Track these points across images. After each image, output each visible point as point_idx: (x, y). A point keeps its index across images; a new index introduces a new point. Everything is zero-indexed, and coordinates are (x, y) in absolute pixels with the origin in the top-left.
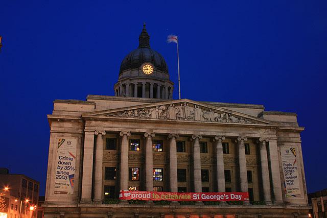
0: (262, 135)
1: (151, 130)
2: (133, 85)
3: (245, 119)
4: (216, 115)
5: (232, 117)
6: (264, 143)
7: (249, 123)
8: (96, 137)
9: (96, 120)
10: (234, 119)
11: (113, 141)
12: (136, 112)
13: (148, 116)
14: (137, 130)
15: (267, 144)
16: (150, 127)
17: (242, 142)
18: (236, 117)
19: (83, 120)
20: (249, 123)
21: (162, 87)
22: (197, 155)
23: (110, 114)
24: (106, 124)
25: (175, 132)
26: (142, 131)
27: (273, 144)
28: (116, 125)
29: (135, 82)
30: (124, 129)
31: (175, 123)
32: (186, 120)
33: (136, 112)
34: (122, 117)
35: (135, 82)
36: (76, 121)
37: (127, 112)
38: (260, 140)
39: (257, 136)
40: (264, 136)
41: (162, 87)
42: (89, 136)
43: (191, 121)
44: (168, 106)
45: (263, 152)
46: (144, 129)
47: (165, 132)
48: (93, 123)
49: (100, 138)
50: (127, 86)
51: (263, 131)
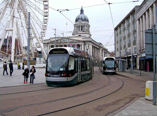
0: (80, 43)
7: (77, 41)
8: (50, 46)
10: (75, 41)
15: (81, 45)
19: (47, 44)
20: (77, 41)
21: (84, 26)
24: (51, 44)
27: (83, 46)
29: (77, 25)
34: (53, 42)
35: (77, 25)
36: (47, 44)
41: (84, 26)
45: (81, 47)
48: (49, 44)
49: (50, 47)
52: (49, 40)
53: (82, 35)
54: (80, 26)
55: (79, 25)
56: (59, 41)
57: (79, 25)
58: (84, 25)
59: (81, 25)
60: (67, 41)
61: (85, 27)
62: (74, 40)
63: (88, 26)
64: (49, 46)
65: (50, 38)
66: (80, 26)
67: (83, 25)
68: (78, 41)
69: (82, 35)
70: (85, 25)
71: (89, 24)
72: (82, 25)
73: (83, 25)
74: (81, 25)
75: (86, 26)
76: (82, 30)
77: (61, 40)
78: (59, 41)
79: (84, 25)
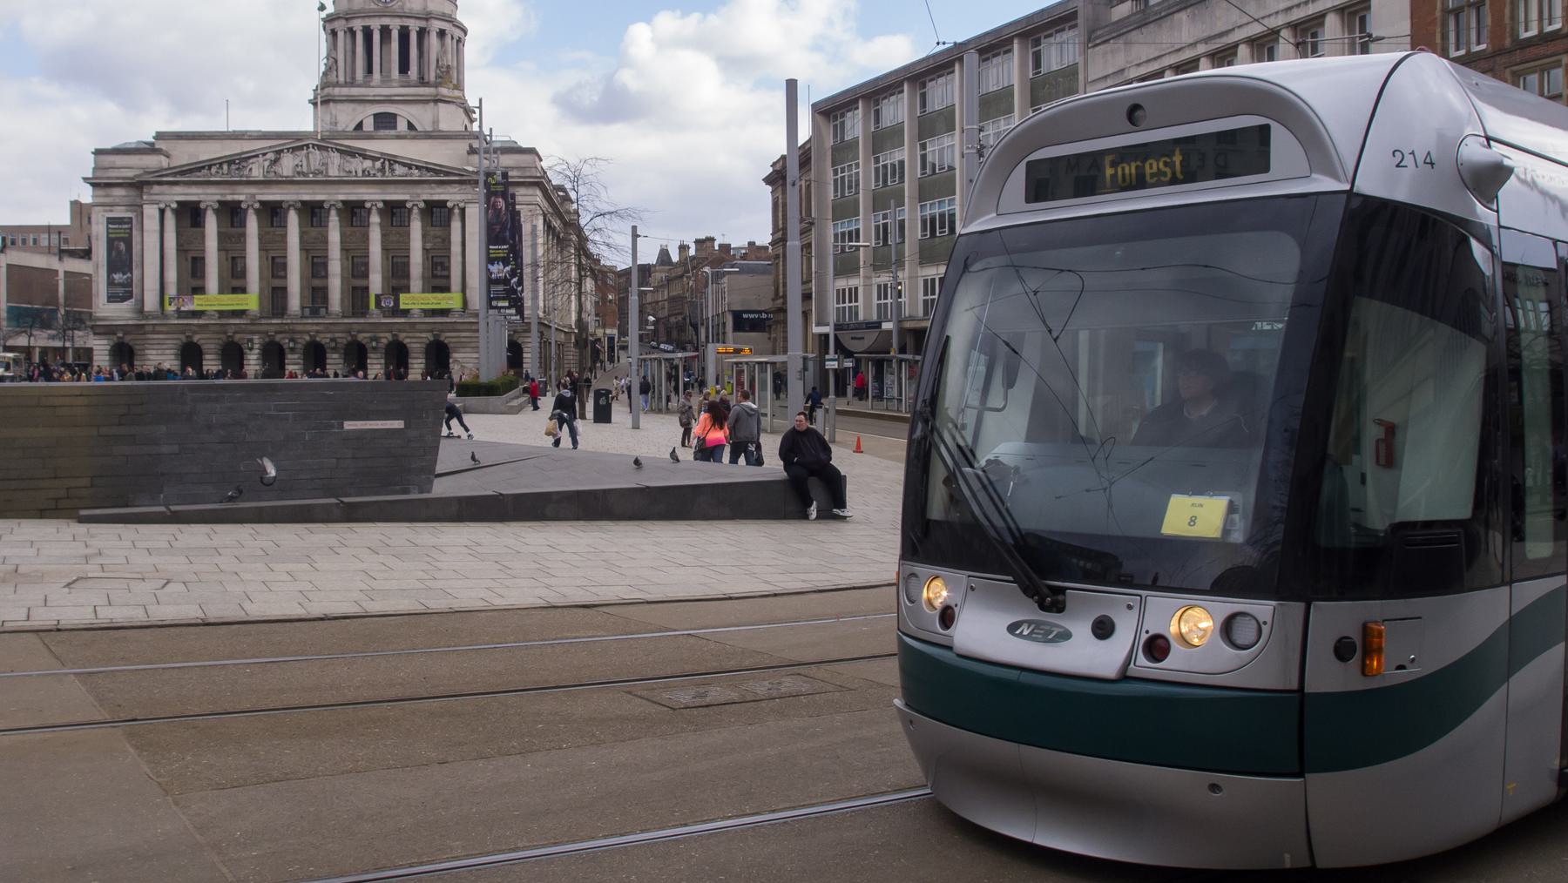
0: (451, 195)
1: (253, 196)
2: (352, 32)
3: (418, 167)
4: (368, 163)
5: (396, 166)
6: (456, 211)
8: (162, 212)
9: (160, 183)
10: (399, 170)
11: (190, 215)
12: (225, 167)
13: (246, 172)
14: (229, 198)
15: (463, 211)
16: (252, 190)
17: (415, 210)
18: (404, 165)
19: (138, 185)
22: (334, 236)
23: (182, 173)
24: (178, 189)
25: (295, 198)
26: (237, 198)
28: (194, 190)
29: (358, 25)
30: (208, 196)
31: (290, 182)
32: (311, 177)
33: (225, 167)
35: (358, 25)
37: (210, 167)
38: (449, 205)
39: (443, 197)
40: (458, 197)
41: (422, 33)
42: (151, 212)
43: (320, 178)
44: (279, 152)
45: (456, 225)
46: (241, 195)
47: (278, 198)
48: (156, 189)
50: (341, 35)
51: (455, 188)
52: (150, 149)
53: (404, 113)
54: (385, 31)
55: (375, 24)
56: (257, 171)
57: (375, 24)
58: (423, 24)
59: (395, 25)
60: (335, 165)
61: (433, 39)
62: (392, 160)
63: (458, 33)
64: (151, 212)
65: (160, 136)
66: (385, 31)
67: (414, 26)
68: (437, 172)
69: (404, 113)
70: (437, 25)
71: (460, 17)
72: (407, 22)
73: (414, 26)
74: (395, 25)
75: (442, 34)
76: (404, 67)
77: (275, 162)
78: (257, 171)
79: (423, 24)
